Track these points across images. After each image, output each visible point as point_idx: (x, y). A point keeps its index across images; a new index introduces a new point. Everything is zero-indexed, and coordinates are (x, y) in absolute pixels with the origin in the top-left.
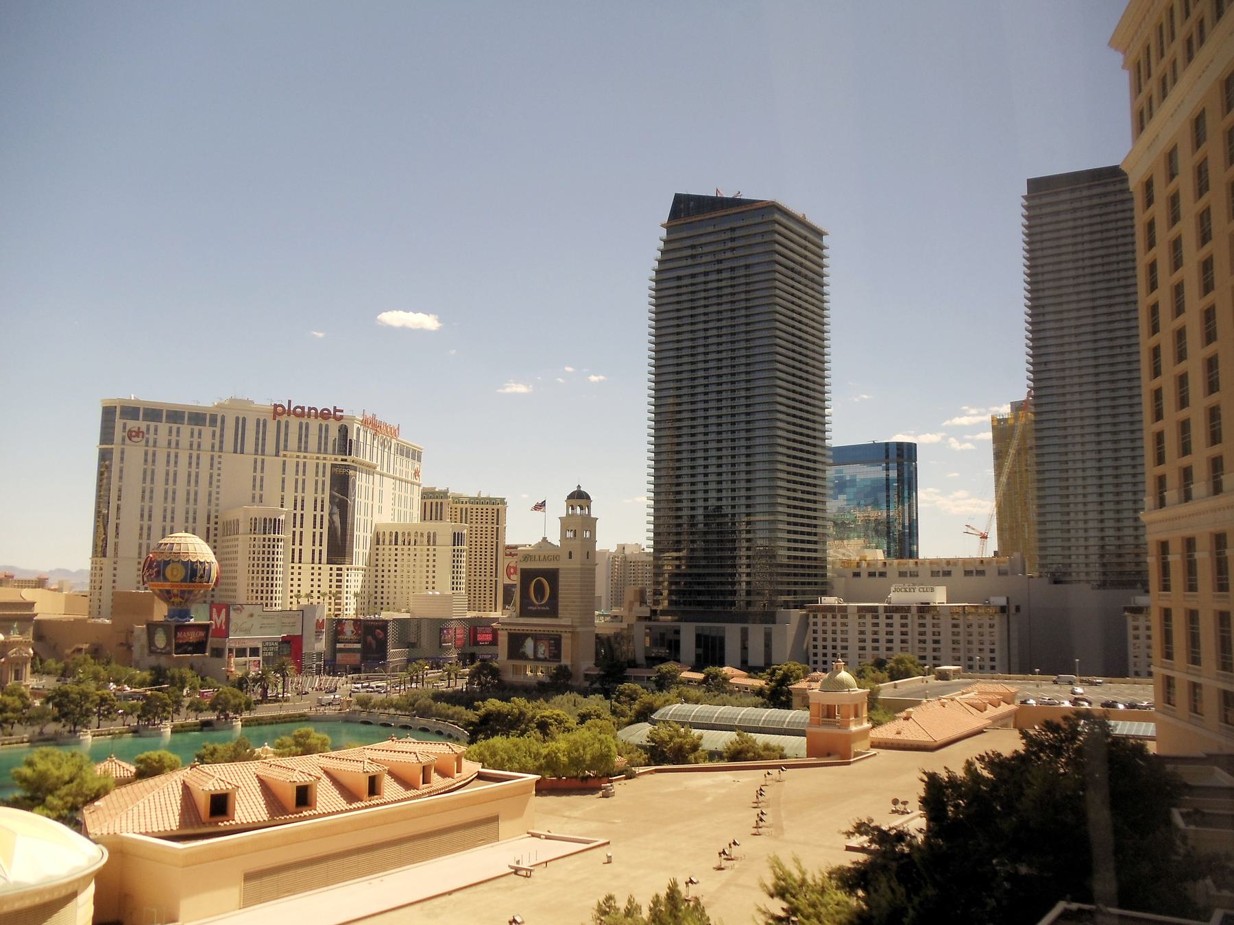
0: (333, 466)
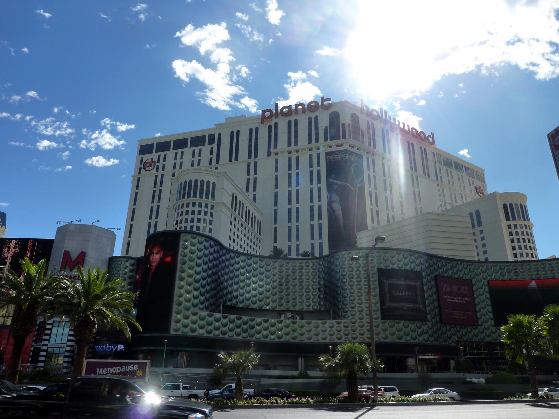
0: (328, 154)
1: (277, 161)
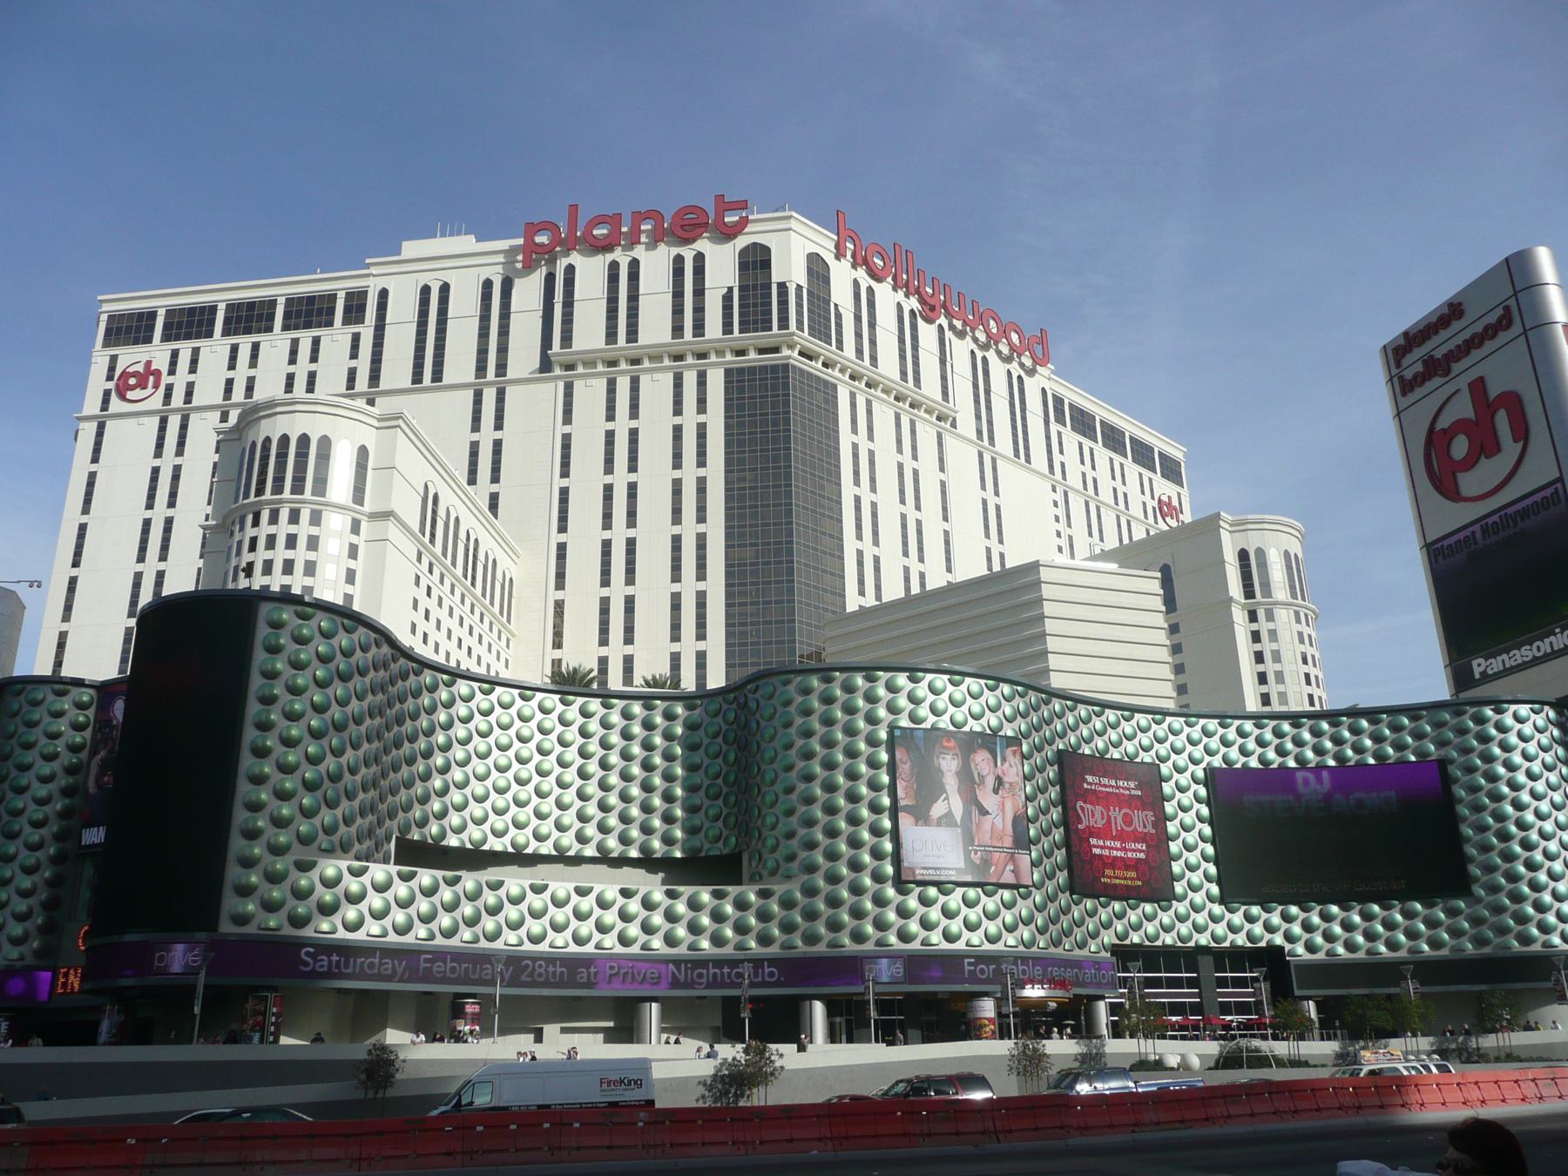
1: (569, 388)
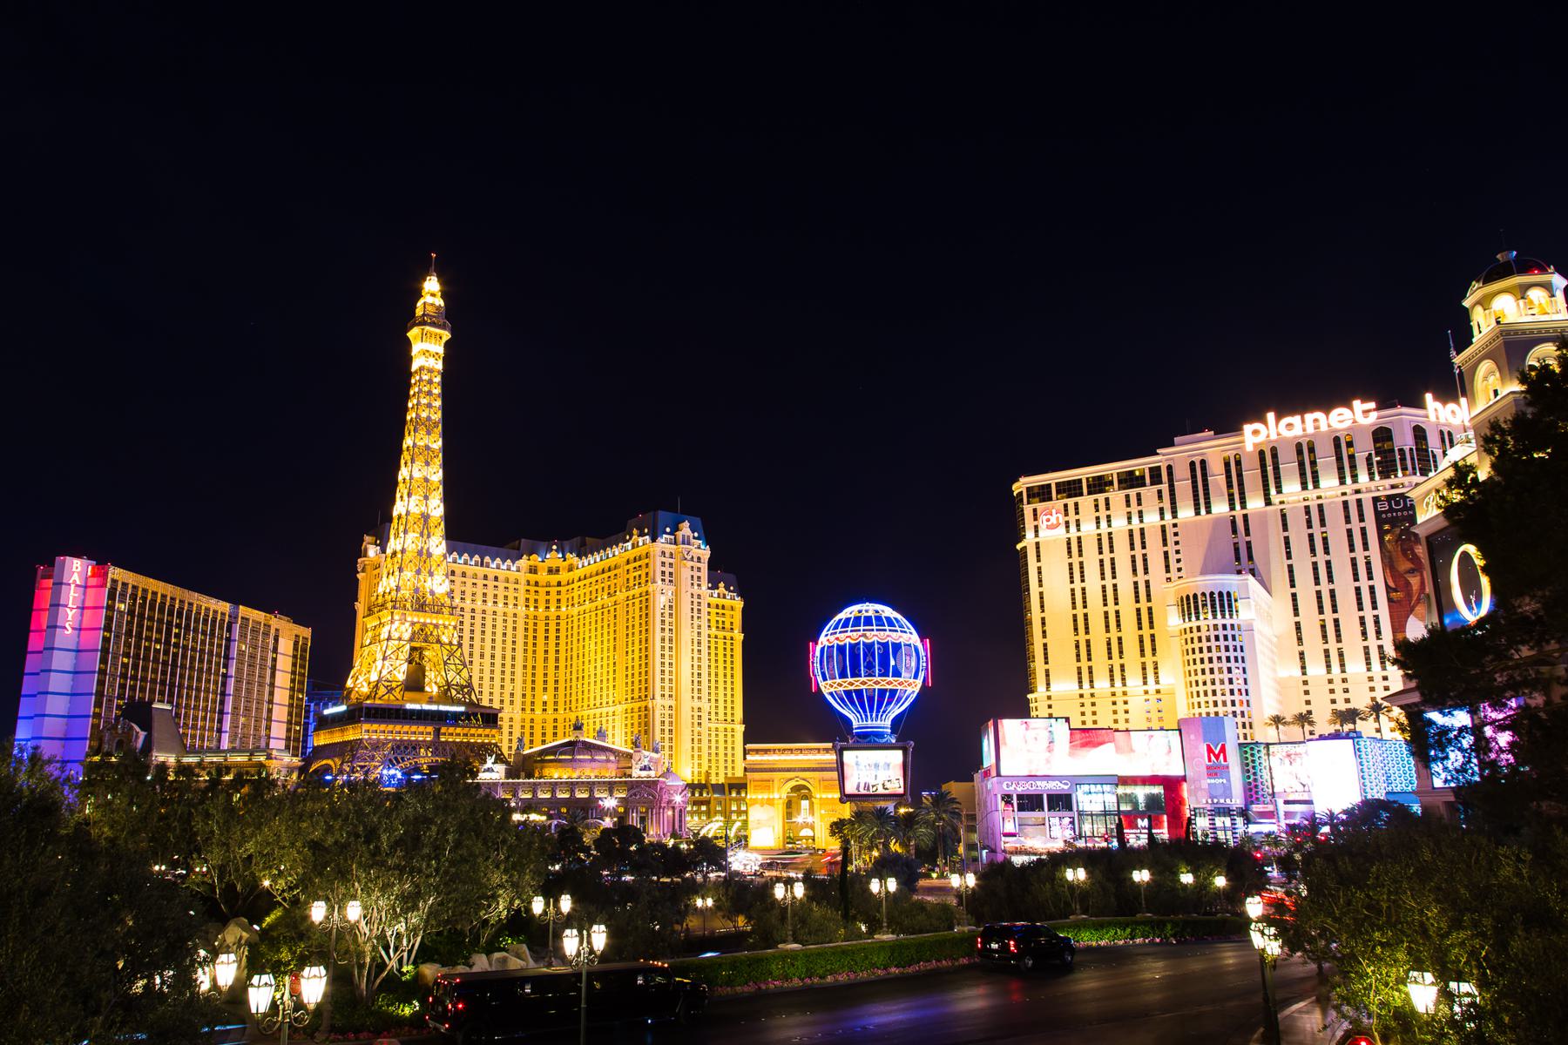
0: (1376, 500)
